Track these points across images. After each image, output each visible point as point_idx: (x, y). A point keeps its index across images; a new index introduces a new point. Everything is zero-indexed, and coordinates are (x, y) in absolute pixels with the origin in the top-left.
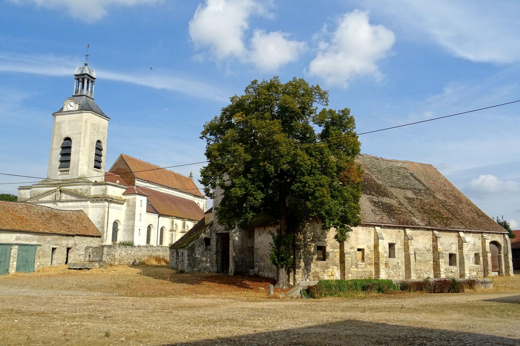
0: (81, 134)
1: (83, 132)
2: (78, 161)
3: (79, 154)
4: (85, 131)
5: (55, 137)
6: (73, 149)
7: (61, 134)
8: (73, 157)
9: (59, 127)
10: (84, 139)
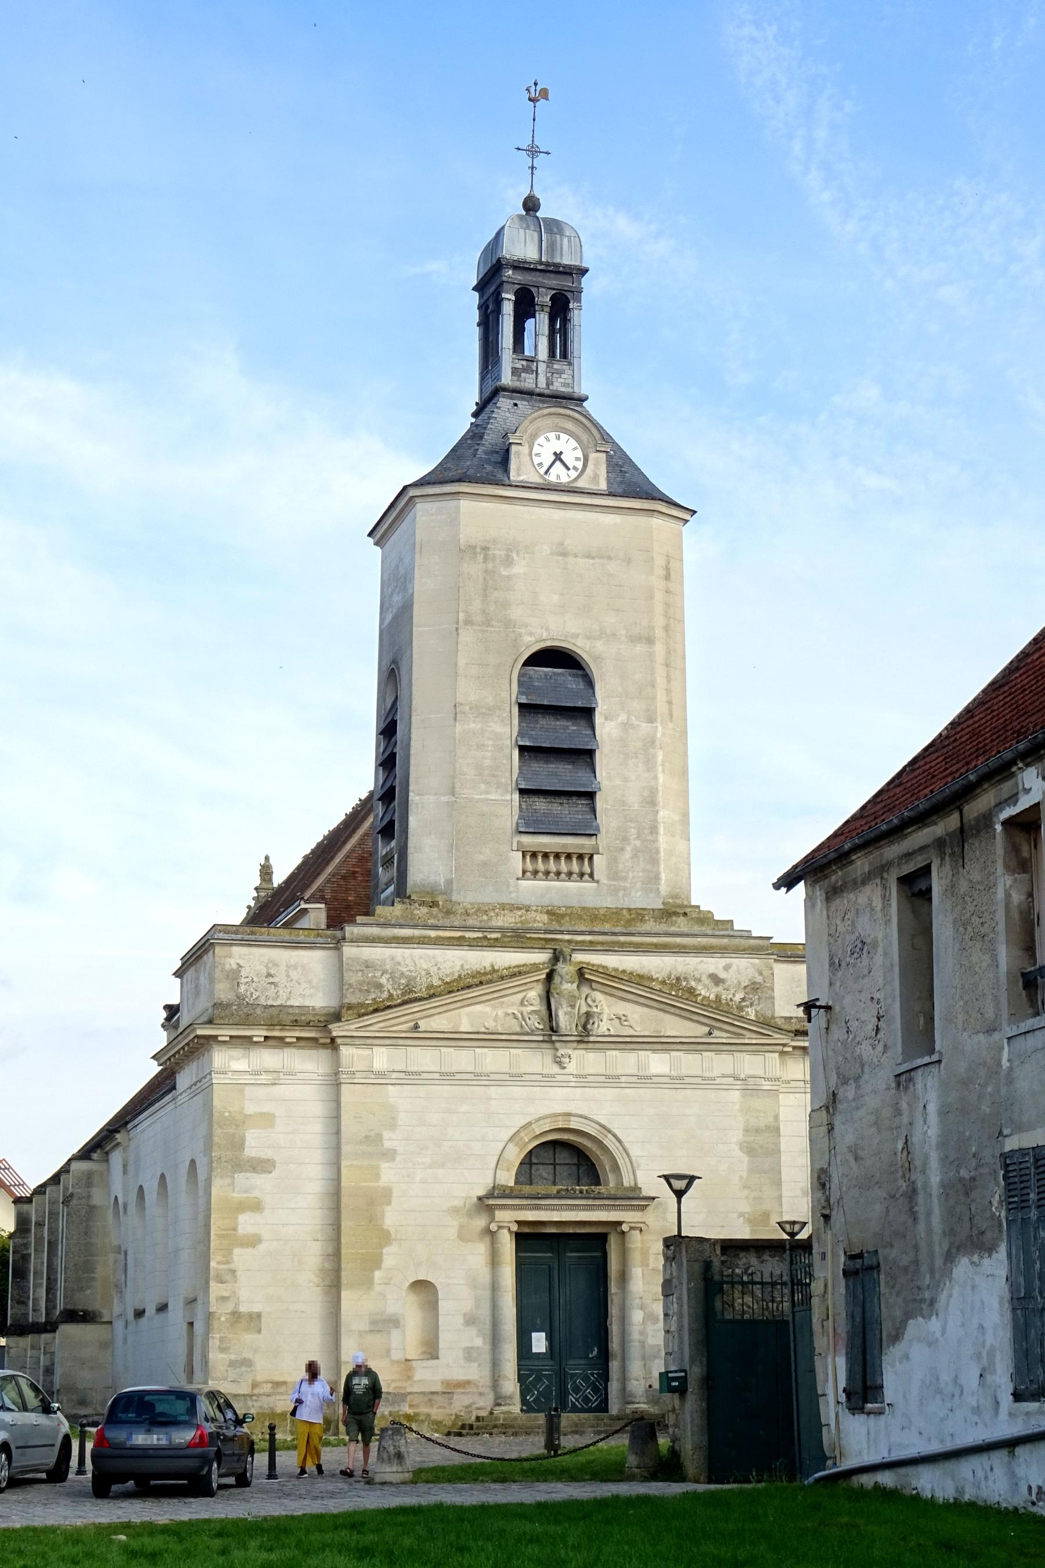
0: (650, 641)
1: (659, 633)
2: (651, 801)
3: (650, 764)
4: (667, 629)
5: (467, 636)
7: (508, 623)
10: (669, 678)
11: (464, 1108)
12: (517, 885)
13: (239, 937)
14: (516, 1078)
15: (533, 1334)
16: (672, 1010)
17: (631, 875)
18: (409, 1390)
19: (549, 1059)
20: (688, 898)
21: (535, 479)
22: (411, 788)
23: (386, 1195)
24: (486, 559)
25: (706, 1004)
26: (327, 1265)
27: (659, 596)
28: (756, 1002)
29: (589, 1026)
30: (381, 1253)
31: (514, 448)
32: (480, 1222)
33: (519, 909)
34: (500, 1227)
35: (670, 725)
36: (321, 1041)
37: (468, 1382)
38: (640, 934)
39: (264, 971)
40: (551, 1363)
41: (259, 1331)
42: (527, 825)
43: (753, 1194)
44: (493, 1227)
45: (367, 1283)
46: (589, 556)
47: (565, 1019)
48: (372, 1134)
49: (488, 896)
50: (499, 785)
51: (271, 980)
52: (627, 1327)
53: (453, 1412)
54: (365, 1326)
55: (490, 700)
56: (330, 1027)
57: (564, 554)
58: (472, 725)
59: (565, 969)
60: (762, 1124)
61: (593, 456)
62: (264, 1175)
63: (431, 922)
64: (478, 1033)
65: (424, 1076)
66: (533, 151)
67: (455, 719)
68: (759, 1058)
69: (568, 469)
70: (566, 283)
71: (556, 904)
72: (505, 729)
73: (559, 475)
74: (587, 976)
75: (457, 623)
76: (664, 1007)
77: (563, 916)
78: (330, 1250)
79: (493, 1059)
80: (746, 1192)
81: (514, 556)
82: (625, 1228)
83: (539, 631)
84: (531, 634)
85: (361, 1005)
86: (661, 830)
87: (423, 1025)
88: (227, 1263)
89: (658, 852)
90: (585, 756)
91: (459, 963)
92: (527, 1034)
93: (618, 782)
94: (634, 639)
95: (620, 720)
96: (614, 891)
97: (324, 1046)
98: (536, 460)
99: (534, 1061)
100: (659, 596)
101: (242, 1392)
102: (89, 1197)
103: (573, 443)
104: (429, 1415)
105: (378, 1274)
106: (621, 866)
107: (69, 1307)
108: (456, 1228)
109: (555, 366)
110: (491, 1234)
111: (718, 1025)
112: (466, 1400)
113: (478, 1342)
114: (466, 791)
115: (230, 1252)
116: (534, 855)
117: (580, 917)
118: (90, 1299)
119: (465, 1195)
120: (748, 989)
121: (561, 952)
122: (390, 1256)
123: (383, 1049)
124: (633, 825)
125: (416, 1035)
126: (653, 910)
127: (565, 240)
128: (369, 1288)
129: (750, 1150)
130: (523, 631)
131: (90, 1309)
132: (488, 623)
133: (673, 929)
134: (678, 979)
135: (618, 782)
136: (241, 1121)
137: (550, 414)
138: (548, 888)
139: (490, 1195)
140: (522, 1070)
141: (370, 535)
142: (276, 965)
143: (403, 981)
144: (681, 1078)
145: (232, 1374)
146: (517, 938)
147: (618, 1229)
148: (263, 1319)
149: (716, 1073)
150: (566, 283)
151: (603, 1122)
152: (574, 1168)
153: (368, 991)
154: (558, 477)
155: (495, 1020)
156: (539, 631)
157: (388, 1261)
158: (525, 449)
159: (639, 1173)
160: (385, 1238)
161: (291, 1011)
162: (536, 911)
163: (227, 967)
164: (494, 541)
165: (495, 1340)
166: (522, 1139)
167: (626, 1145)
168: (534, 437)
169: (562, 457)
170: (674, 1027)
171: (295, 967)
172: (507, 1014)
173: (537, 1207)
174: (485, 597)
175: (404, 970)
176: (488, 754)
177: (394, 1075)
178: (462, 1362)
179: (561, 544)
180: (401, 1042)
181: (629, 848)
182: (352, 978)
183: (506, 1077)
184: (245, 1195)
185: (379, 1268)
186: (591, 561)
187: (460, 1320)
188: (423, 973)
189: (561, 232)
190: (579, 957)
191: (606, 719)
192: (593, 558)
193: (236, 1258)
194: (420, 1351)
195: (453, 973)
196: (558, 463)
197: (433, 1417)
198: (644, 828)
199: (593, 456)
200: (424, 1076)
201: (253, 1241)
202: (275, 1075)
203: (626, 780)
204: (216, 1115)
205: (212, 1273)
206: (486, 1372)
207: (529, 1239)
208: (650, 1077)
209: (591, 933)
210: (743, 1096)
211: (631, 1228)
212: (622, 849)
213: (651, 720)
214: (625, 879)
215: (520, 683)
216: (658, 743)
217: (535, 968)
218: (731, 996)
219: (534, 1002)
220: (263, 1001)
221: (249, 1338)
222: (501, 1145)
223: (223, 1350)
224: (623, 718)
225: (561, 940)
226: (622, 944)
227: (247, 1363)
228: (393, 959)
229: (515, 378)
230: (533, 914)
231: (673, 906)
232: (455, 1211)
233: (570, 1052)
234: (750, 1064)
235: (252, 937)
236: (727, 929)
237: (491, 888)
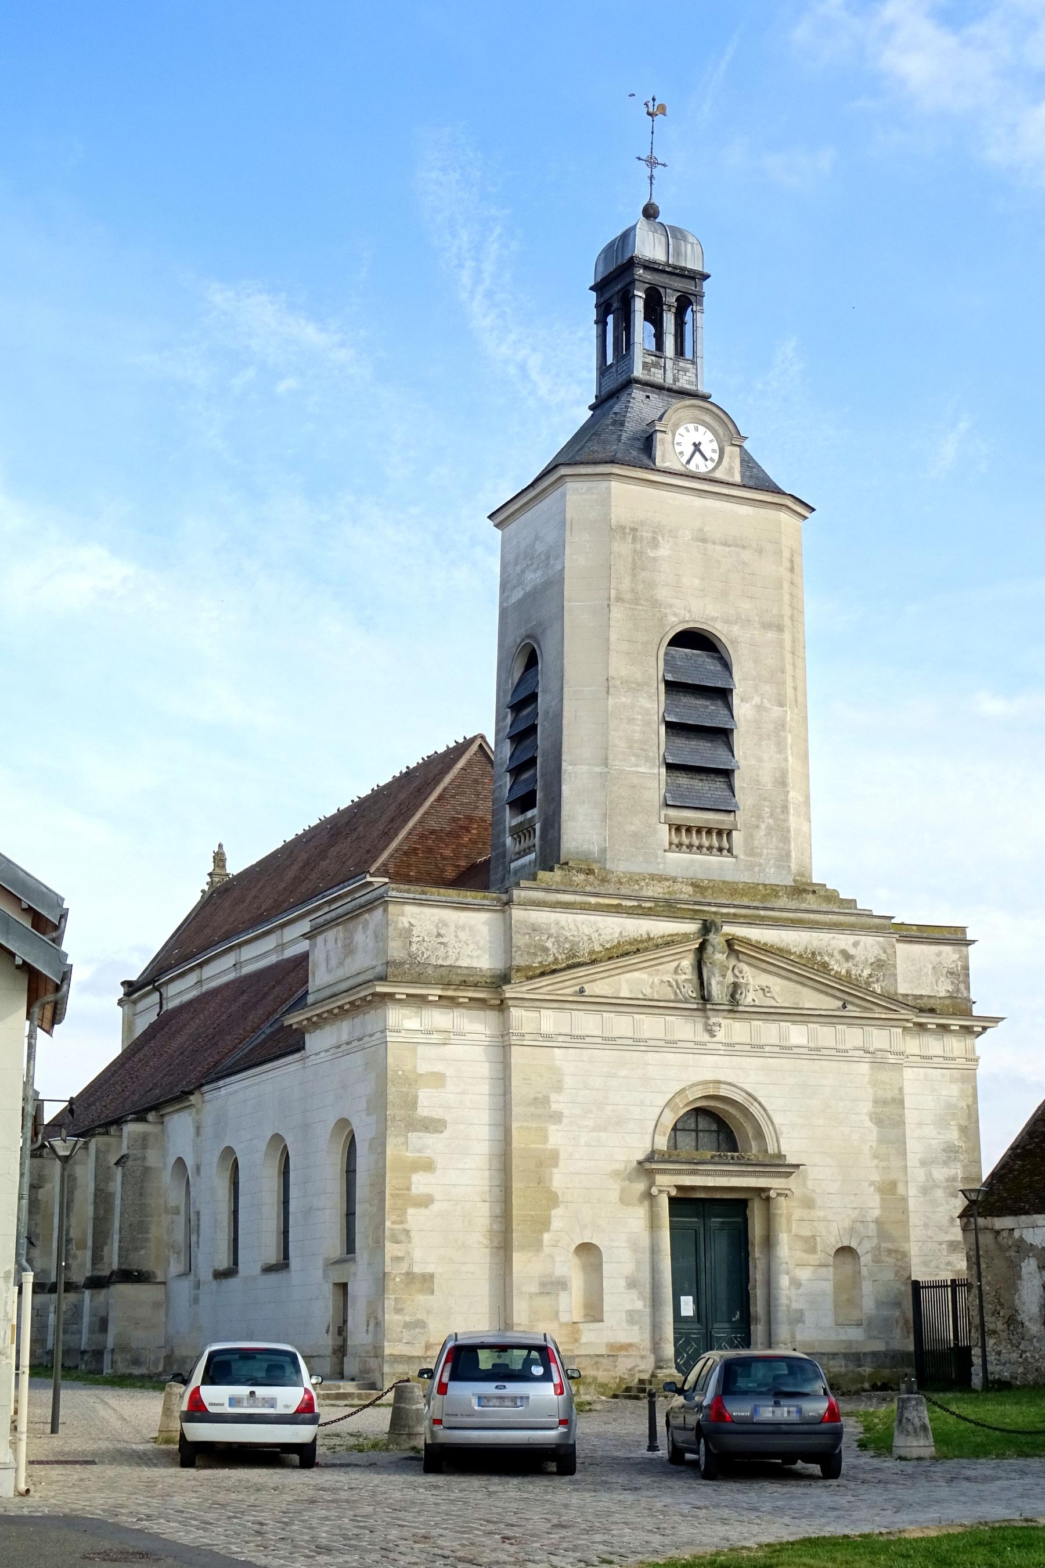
0: (780, 629)
1: (787, 622)
2: (782, 782)
4: (792, 618)
5: (617, 613)
6: (743, 708)
7: (655, 603)
8: (749, 754)
9: (638, 554)
11: (624, 1072)
12: (664, 857)
13: (411, 896)
14: (671, 1044)
15: (682, 1298)
16: (810, 983)
17: (765, 851)
18: (576, 1353)
19: (700, 1027)
20: (811, 877)
21: (677, 467)
22: (564, 757)
23: (553, 1158)
24: (634, 539)
25: (838, 977)
26: (495, 1227)
27: (786, 586)
28: (882, 978)
29: (737, 996)
30: (549, 1217)
31: (659, 435)
32: (640, 1186)
33: (667, 880)
34: (660, 1191)
35: (796, 711)
36: (493, 1002)
37: (630, 1345)
38: (781, 910)
39: (435, 931)
40: (698, 1326)
41: (432, 1292)
42: (674, 798)
43: (884, 1164)
44: (654, 1191)
45: (537, 1245)
46: (725, 544)
47: (717, 989)
48: (540, 1096)
49: (638, 866)
50: (647, 759)
51: (441, 940)
52: (772, 1291)
53: (618, 1375)
54: (534, 1288)
55: (639, 676)
56: (504, 988)
57: (704, 540)
58: (624, 699)
59: (716, 939)
60: (889, 1095)
61: (728, 449)
62: (435, 1135)
63: (588, 889)
64: (638, 999)
65: (588, 1040)
66: (652, 162)
67: (608, 693)
68: (885, 1033)
69: (706, 459)
70: (688, 286)
71: (700, 877)
72: (651, 706)
73: (699, 466)
74: (736, 947)
75: (609, 599)
76: (803, 981)
77: (706, 888)
78: (498, 1211)
79: (651, 1025)
80: (876, 1162)
81: (660, 539)
82: (773, 1194)
83: (682, 612)
84: (675, 615)
85: (529, 968)
86: (791, 811)
87: (589, 989)
88: (402, 1222)
89: (789, 831)
90: (723, 735)
91: (618, 930)
92: (682, 1002)
93: (753, 762)
94: (766, 626)
95: (754, 703)
96: (750, 867)
97: (492, 1007)
98: (678, 449)
99: (686, 1028)
100: (786, 586)
101: (416, 1354)
102: (144, 1158)
103: (710, 436)
104: (595, 1378)
105: (546, 1236)
106: (756, 843)
107: (123, 1267)
108: (618, 1192)
109: (681, 364)
110: (649, 1196)
111: (851, 999)
112: (629, 1363)
113: (639, 1305)
114: (617, 763)
115: (404, 1213)
116: (678, 829)
117: (722, 891)
118: (145, 1260)
119: (625, 1159)
120: (874, 966)
121: (713, 923)
122: (558, 1218)
123: (550, 1012)
124: (767, 804)
125: (581, 1000)
126: (786, 887)
127: (689, 246)
128: (539, 1250)
129: (878, 1121)
130: (668, 611)
131: (144, 1270)
132: (636, 601)
133: (804, 906)
134: (813, 953)
135: (753, 762)
136: (413, 1080)
137: (692, 406)
138: (692, 860)
139: (650, 1158)
140: (676, 1037)
141: (490, 517)
142: (445, 925)
143: (567, 946)
144: (818, 1049)
145: (406, 1336)
146: (668, 908)
147: (763, 1195)
148: (436, 1281)
149: (848, 1046)
150: (688, 286)
151: (750, 1090)
152: (715, 1135)
153: (535, 954)
154: (697, 466)
155: (652, 987)
156: (682, 612)
157: (556, 1224)
158: (668, 437)
159: (782, 1141)
160: (553, 1200)
161: (459, 971)
162: (682, 882)
163: (400, 924)
164: (642, 523)
165: (655, 1303)
166: (677, 1104)
167: (770, 1112)
168: (677, 426)
169: (701, 447)
170: (811, 1000)
171: (463, 928)
172: (662, 982)
173: (694, 1172)
174: (634, 575)
175: (568, 934)
176: (637, 728)
177: (561, 1038)
178: (625, 1325)
179: (701, 530)
180: (567, 1006)
181: (763, 826)
182: (520, 940)
183: (662, 1043)
184: (418, 1155)
185: (548, 1230)
186: (727, 549)
187: (622, 1283)
188: (585, 938)
189: (684, 239)
190: (727, 929)
191: (742, 701)
192: (729, 546)
193: (409, 1218)
194: (582, 1314)
195: (612, 940)
196: (697, 453)
197: (600, 1380)
198: (776, 807)
199: (728, 449)
200: (588, 1040)
201: (426, 1201)
202: (445, 1035)
203: (760, 760)
204: (390, 1074)
205: (387, 1233)
206: (647, 1336)
207: (684, 1204)
208: (790, 1048)
209: (735, 906)
210: (872, 1069)
211: (779, 1195)
212: (758, 827)
213: (781, 704)
214: (761, 855)
215: (666, 661)
216: (788, 727)
217: (686, 938)
218: (859, 972)
219: (687, 971)
220: (433, 961)
221: (421, 1298)
222: (658, 1111)
223: (398, 1311)
224: (757, 700)
225: (708, 912)
226: (763, 918)
227: (421, 1324)
228: (557, 924)
229: (646, 372)
230: (680, 886)
231: (803, 884)
232: (615, 1174)
233: (721, 1020)
234: (879, 1038)
235: (423, 897)
236: (851, 908)
237: (641, 858)
